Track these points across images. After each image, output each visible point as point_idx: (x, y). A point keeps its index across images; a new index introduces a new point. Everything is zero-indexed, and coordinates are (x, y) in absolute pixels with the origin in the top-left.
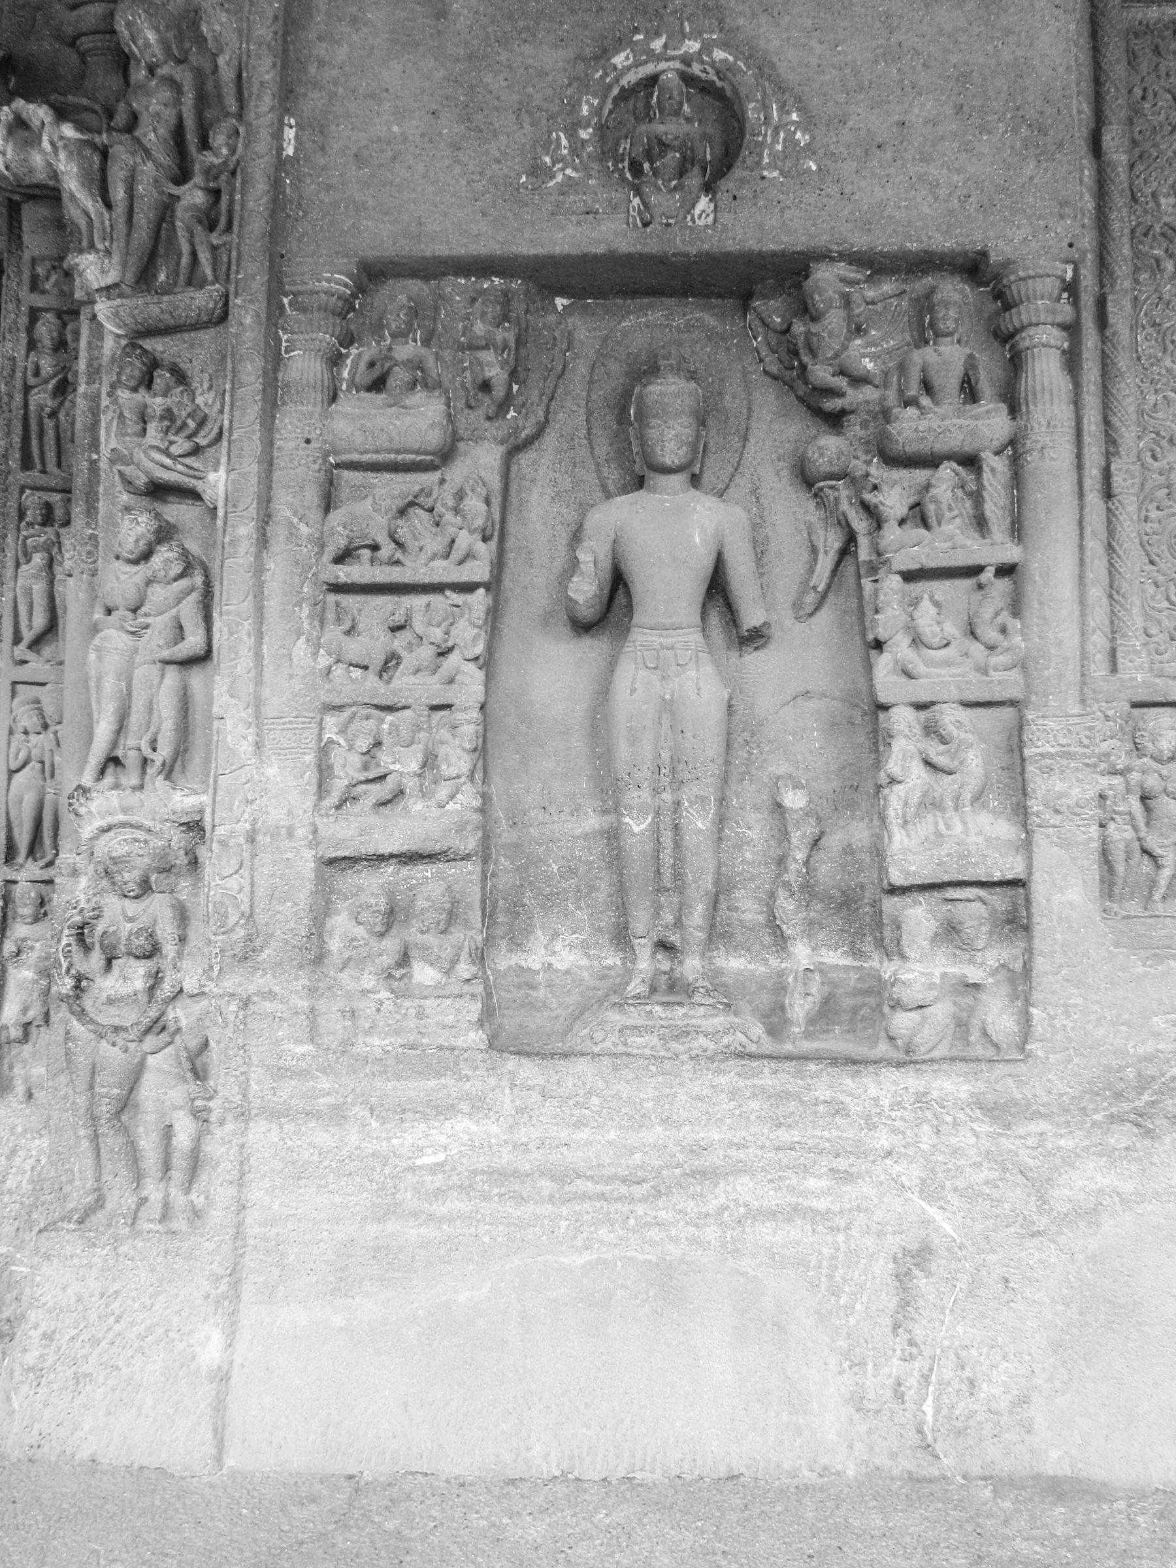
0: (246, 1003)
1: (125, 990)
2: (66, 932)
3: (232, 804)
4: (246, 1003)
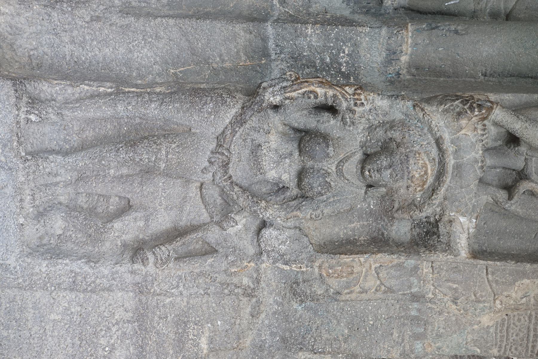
0: (249, 293)
1: (267, 163)
2: (331, 93)
3: (454, 282)
4: (249, 293)
